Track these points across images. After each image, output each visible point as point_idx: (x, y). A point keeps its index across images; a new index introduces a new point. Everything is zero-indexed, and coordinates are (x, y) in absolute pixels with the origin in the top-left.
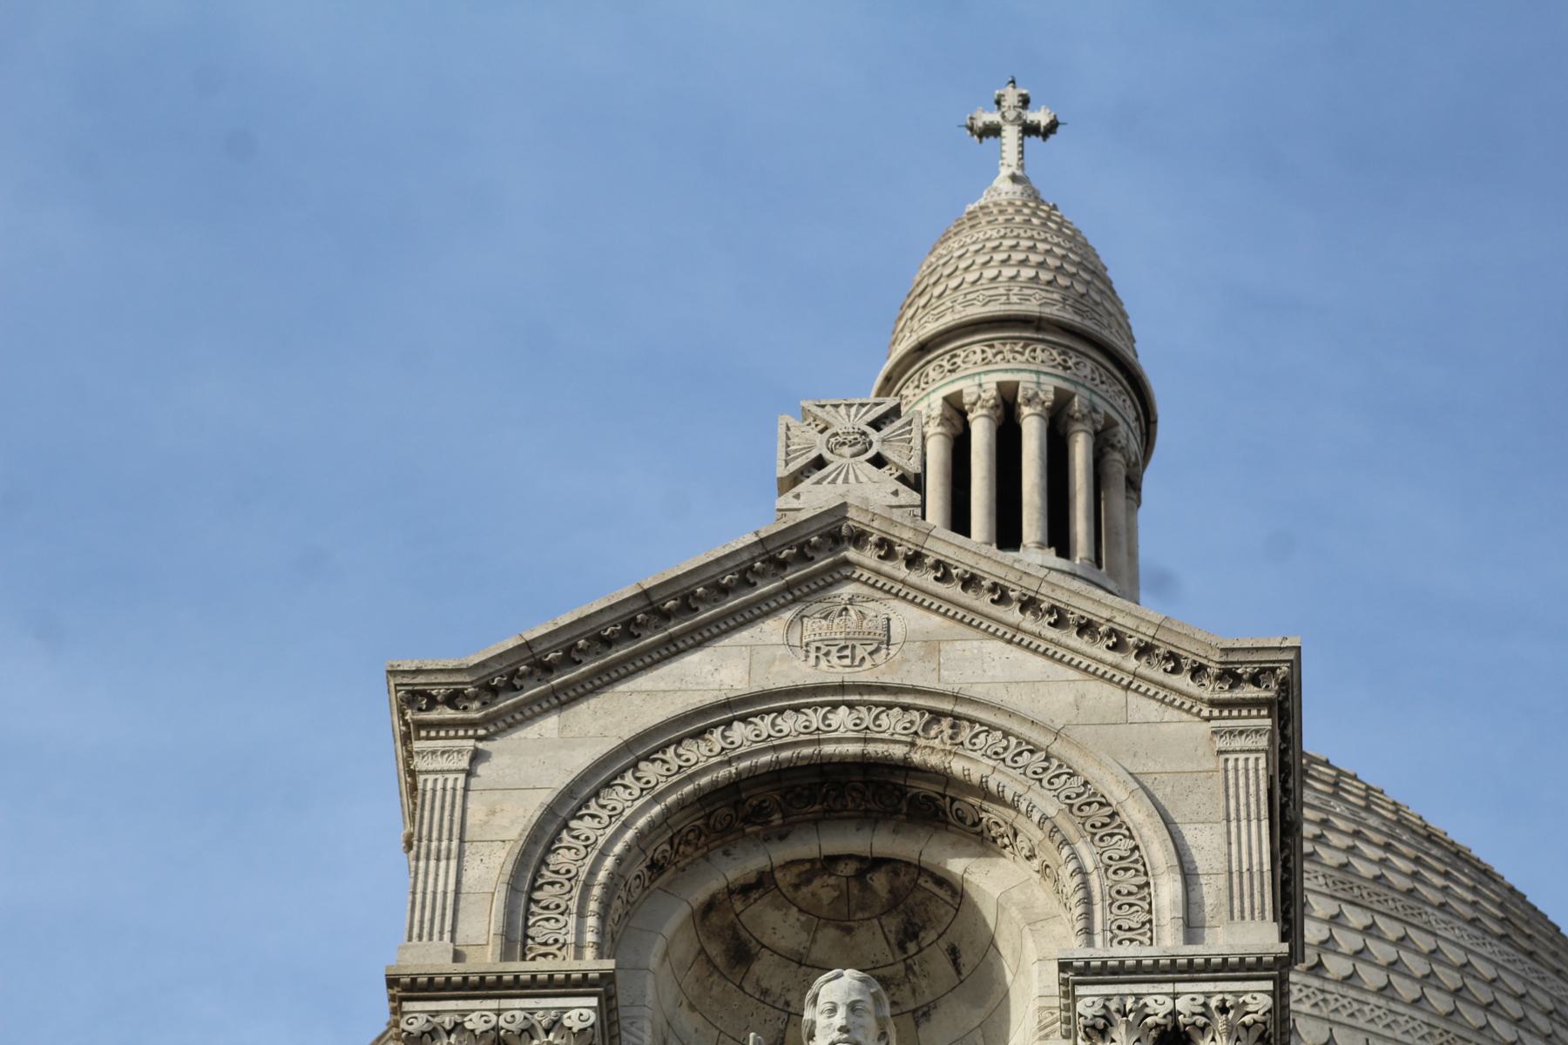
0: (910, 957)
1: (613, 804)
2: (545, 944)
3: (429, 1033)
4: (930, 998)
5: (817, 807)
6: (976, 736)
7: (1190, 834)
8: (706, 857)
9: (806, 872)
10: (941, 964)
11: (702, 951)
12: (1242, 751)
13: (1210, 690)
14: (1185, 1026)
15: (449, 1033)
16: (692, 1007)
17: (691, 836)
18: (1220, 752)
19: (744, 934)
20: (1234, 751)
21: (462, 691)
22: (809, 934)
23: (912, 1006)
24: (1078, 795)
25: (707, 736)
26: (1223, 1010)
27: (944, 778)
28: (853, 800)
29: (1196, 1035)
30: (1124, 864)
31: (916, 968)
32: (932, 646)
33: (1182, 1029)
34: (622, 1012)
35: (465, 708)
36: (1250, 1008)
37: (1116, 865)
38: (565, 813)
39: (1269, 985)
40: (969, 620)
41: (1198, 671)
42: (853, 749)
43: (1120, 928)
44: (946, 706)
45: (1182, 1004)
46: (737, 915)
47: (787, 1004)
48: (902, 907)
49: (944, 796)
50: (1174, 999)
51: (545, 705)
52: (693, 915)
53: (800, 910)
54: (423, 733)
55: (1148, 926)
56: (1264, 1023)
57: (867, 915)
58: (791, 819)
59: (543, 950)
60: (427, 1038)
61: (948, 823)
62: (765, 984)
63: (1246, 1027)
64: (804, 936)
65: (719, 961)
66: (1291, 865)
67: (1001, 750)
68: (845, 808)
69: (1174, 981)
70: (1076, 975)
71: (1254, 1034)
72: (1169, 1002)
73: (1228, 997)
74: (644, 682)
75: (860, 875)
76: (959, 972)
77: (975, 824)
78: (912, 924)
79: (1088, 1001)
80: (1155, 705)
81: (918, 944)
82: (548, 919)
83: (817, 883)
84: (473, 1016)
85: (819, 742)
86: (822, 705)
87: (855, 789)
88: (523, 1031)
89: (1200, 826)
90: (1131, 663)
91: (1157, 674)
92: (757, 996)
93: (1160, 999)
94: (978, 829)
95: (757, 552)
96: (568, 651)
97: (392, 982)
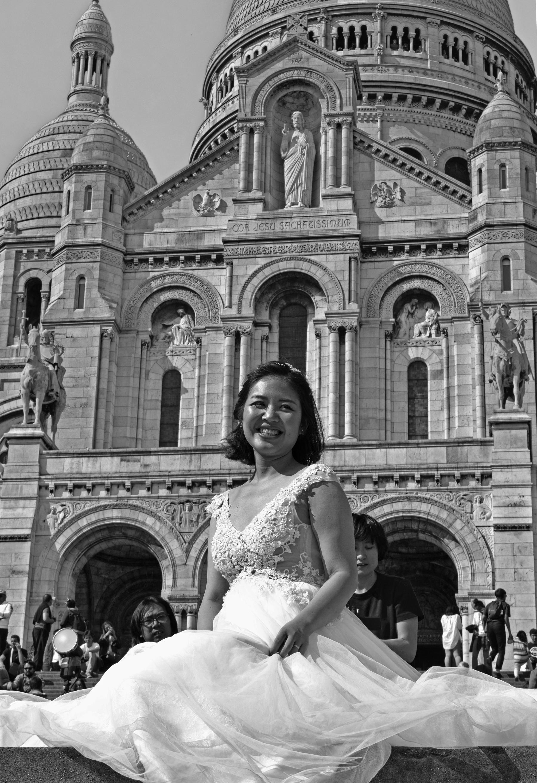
7: (342, 91)
10: (311, 104)
32: (308, 59)
40: (313, 54)
41: (343, 64)
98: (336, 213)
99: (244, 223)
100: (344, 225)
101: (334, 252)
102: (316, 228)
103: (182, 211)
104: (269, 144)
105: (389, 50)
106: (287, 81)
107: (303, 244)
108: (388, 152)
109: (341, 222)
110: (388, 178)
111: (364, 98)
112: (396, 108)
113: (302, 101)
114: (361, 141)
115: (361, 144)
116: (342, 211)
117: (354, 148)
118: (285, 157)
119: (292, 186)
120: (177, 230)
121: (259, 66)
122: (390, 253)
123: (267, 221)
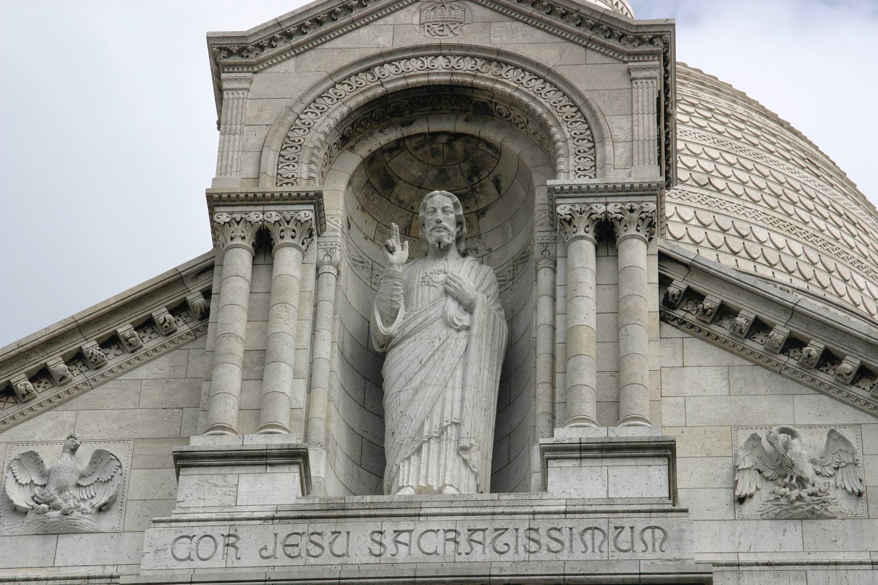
0: (475, 184)
1: (323, 106)
2: (288, 178)
3: (228, 222)
5: (427, 108)
6: (508, 71)
8: (371, 134)
9: (421, 141)
10: (490, 188)
11: (368, 181)
12: (645, 78)
13: (629, 48)
14: (611, 219)
15: (238, 223)
16: (363, 209)
17: (363, 123)
19: (390, 172)
20: (641, 79)
21: (246, 48)
22: (423, 172)
23: (475, 209)
24: (560, 102)
26: (632, 211)
27: (491, 90)
28: (446, 104)
29: (617, 223)
30: (582, 137)
31: (478, 189)
33: (610, 220)
34: (327, 212)
35: (247, 57)
36: (645, 210)
37: (578, 137)
38: (298, 109)
41: (620, 38)
43: (579, 169)
45: (610, 208)
46: (387, 163)
47: (412, 208)
48: (470, 158)
49: (491, 102)
50: (606, 205)
53: (419, 160)
54: (226, 70)
55: (593, 168)
56: (652, 217)
57: (453, 163)
58: (414, 114)
59: (286, 181)
60: (227, 225)
61: (494, 116)
62: (401, 198)
63: (643, 220)
65: (377, 186)
66: (670, 136)
67: (520, 79)
68: (441, 108)
69: (606, 196)
70: (556, 193)
71: (647, 222)
73: (633, 204)
74: (339, 42)
75: (449, 143)
76: (499, 192)
77: (507, 116)
78: (476, 167)
79: (562, 206)
81: (479, 177)
82: (288, 165)
83: (427, 148)
84: (252, 215)
85: (428, 74)
87: (446, 98)
88: (276, 222)
90: (588, 34)
91: (601, 39)
92: (397, 204)
93: (599, 205)
94: (509, 119)
96: (300, 27)
99: (219, 530)
102: (523, 555)
106: (407, 92)
108: (800, 330)
116: (628, 501)
117: (664, 318)
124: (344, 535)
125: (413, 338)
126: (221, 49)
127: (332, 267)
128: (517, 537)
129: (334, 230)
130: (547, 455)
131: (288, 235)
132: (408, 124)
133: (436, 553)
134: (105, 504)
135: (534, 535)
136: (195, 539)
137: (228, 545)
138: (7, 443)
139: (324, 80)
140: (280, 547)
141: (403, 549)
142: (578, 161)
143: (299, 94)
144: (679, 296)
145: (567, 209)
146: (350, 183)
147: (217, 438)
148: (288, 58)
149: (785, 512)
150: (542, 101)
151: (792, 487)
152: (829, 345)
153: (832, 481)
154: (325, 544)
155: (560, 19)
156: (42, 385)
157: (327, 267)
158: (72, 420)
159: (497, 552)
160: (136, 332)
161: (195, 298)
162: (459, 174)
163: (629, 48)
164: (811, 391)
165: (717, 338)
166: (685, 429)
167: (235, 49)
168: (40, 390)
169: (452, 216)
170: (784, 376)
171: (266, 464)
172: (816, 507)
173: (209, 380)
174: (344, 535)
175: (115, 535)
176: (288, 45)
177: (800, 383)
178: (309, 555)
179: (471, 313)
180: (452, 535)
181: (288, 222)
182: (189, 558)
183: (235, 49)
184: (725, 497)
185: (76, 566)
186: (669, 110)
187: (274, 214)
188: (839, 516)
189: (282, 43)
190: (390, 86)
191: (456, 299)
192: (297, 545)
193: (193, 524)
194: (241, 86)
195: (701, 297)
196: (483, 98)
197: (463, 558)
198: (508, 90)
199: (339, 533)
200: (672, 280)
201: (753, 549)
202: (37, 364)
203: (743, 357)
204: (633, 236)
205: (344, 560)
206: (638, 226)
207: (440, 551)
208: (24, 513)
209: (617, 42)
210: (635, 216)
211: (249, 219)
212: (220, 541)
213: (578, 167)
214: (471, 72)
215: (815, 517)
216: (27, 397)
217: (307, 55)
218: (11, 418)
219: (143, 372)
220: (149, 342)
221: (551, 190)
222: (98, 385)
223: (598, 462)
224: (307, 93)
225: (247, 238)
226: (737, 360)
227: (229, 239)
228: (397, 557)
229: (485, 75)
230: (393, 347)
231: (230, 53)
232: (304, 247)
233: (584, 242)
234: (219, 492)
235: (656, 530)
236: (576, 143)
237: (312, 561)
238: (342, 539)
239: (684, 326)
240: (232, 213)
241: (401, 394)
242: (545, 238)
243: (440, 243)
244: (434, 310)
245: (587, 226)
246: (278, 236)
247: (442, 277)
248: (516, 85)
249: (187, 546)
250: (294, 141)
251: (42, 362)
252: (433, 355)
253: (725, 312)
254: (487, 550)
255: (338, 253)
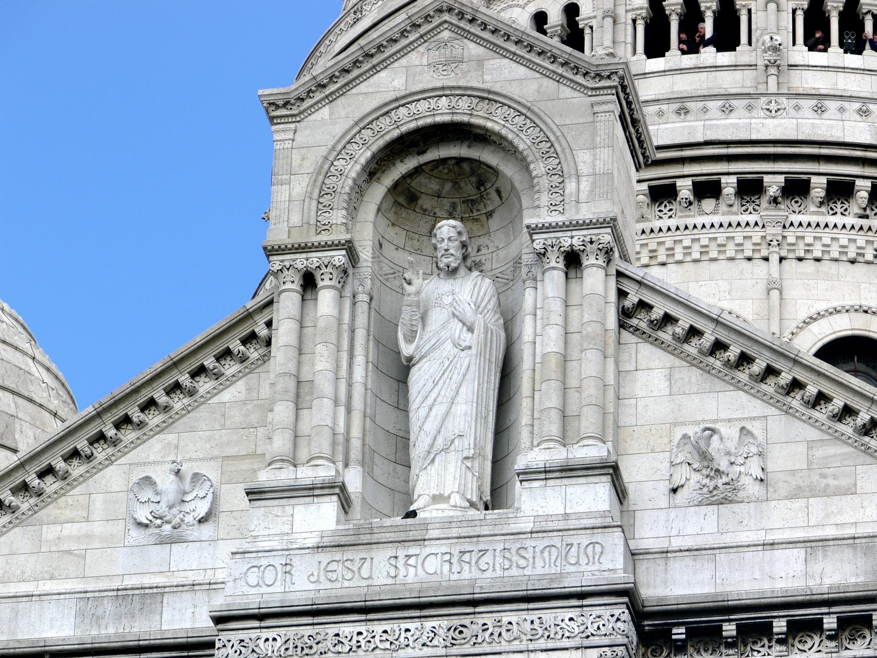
1: (351, 152)
2: (324, 225)
4: (490, 208)
8: (394, 164)
10: (494, 195)
11: (396, 201)
13: (591, 84)
15: (288, 269)
16: (393, 225)
18: (594, 114)
19: (413, 190)
21: (289, 102)
23: (485, 211)
25: (390, 114)
26: (591, 242)
29: (581, 253)
32: (480, 62)
36: (601, 242)
38: (331, 158)
39: (609, 230)
41: (585, 74)
42: (447, 118)
44: (486, 95)
45: (575, 242)
47: (435, 213)
51: (324, 103)
52: (389, 190)
53: (436, 177)
59: (324, 227)
62: (425, 207)
63: (601, 250)
64: (438, 187)
65: (403, 203)
69: (571, 230)
71: (603, 252)
72: (570, 240)
74: (363, 87)
76: (501, 200)
79: (537, 241)
80: (570, 90)
83: (441, 168)
86: (435, 97)
89: (585, 151)
90: (560, 70)
95: (409, 21)
97: (265, 248)
98: (561, 525)
99: (278, 561)
100: (583, 560)
101: (551, 645)
102: (499, 573)
103: (98, 528)
104: (362, 320)
105: (801, 54)
106: (418, 131)
107: (456, 622)
108: (724, 336)
109: (574, 550)
110: (724, 415)
111: (726, 191)
112: (822, 220)
113: (469, 189)
114: (642, 305)
115: (642, 315)
116: (579, 516)
117: (622, 325)
118: (410, 359)
119: (432, 445)
120: (79, 586)
121: (332, 88)
122: (729, 646)
123: (349, 554)
124: (369, 560)
125: (428, 358)
126: (270, 104)
127: (364, 295)
128: (495, 556)
129: (367, 261)
130: (522, 477)
131: (326, 277)
132: (422, 152)
133: (435, 573)
134: (202, 518)
135: (507, 555)
136: (262, 568)
137: (286, 572)
138: (130, 464)
139: (352, 127)
140: (322, 572)
141: (412, 570)
142: (550, 196)
143: (332, 143)
144: (632, 308)
145: (541, 244)
146: (379, 210)
147: (277, 472)
148: (324, 106)
149: (706, 500)
150: (523, 137)
151: (712, 478)
152: (744, 350)
153: (742, 469)
154: (356, 569)
155: (537, 57)
156: (152, 412)
157: (360, 295)
158: (176, 442)
159: (481, 570)
160: (217, 364)
161: (262, 331)
162: (469, 185)
163: (591, 84)
164: (732, 388)
165: (663, 343)
166: (635, 428)
167: (281, 103)
168: (150, 417)
169: (457, 243)
170: (712, 375)
171: (313, 496)
172: (729, 494)
173: (272, 410)
174: (369, 560)
175: (212, 543)
176: (323, 95)
177: (724, 380)
178: (343, 578)
179: (473, 332)
180: (447, 557)
181: (326, 266)
182: (258, 585)
183: (281, 103)
184: (665, 487)
185: (185, 570)
186: (635, 116)
187: (315, 260)
188: (746, 500)
189: (318, 94)
190: (404, 129)
191: (461, 321)
192: (336, 571)
193: (260, 554)
194: (287, 137)
195: (650, 307)
196: (479, 131)
197: (454, 577)
198: (497, 128)
199: (366, 558)
200: (628, 293)
201: (681, 533)
202: (147, 398)
203: (682, 359)
204: (593, 265)
205: (370, 582)
206: (597, 255)
207: (438, 572)
208: (147, 526)
209: (583, 78)
210: (595, 246)
211: (296, 266)
212: (279, 568)
213: (551, 202)
214: (468, 112)
215: (728, 502)
216: (141, 426)
217: (339, 102)
218: (130, 443)
219: (227, 396)
220: (230, 368)
221: (528, 227)
222: (193, 409)
223: (558, 482)
224: (338, 141)
225: (296, 282)
226: (678, 362)
227: (282, 283)
228: (407, 578)
229: (479, 113)
230: (414, 365)
231: (278, 107)
232: (339, 286)
233: (555, 272)
234: (280, 522)
235: (597, 545)
236: (550, 179)
237: (347, 584)
238: (367, 565)
239: (638, 332)
240: (282, 261)
241: (420, 410)
242: (530, 260)
243: (448, 267)
244: (444, 332)
245: (558, 257)
246: (319, 279)
247: (447, 300)
248: (503, 123)
249: (255, 575)
250: (329, 188)
251: (149, 396)
252: (444, 373)
253: (668, 319)
254: (473, 569)
255: (369, 281)
